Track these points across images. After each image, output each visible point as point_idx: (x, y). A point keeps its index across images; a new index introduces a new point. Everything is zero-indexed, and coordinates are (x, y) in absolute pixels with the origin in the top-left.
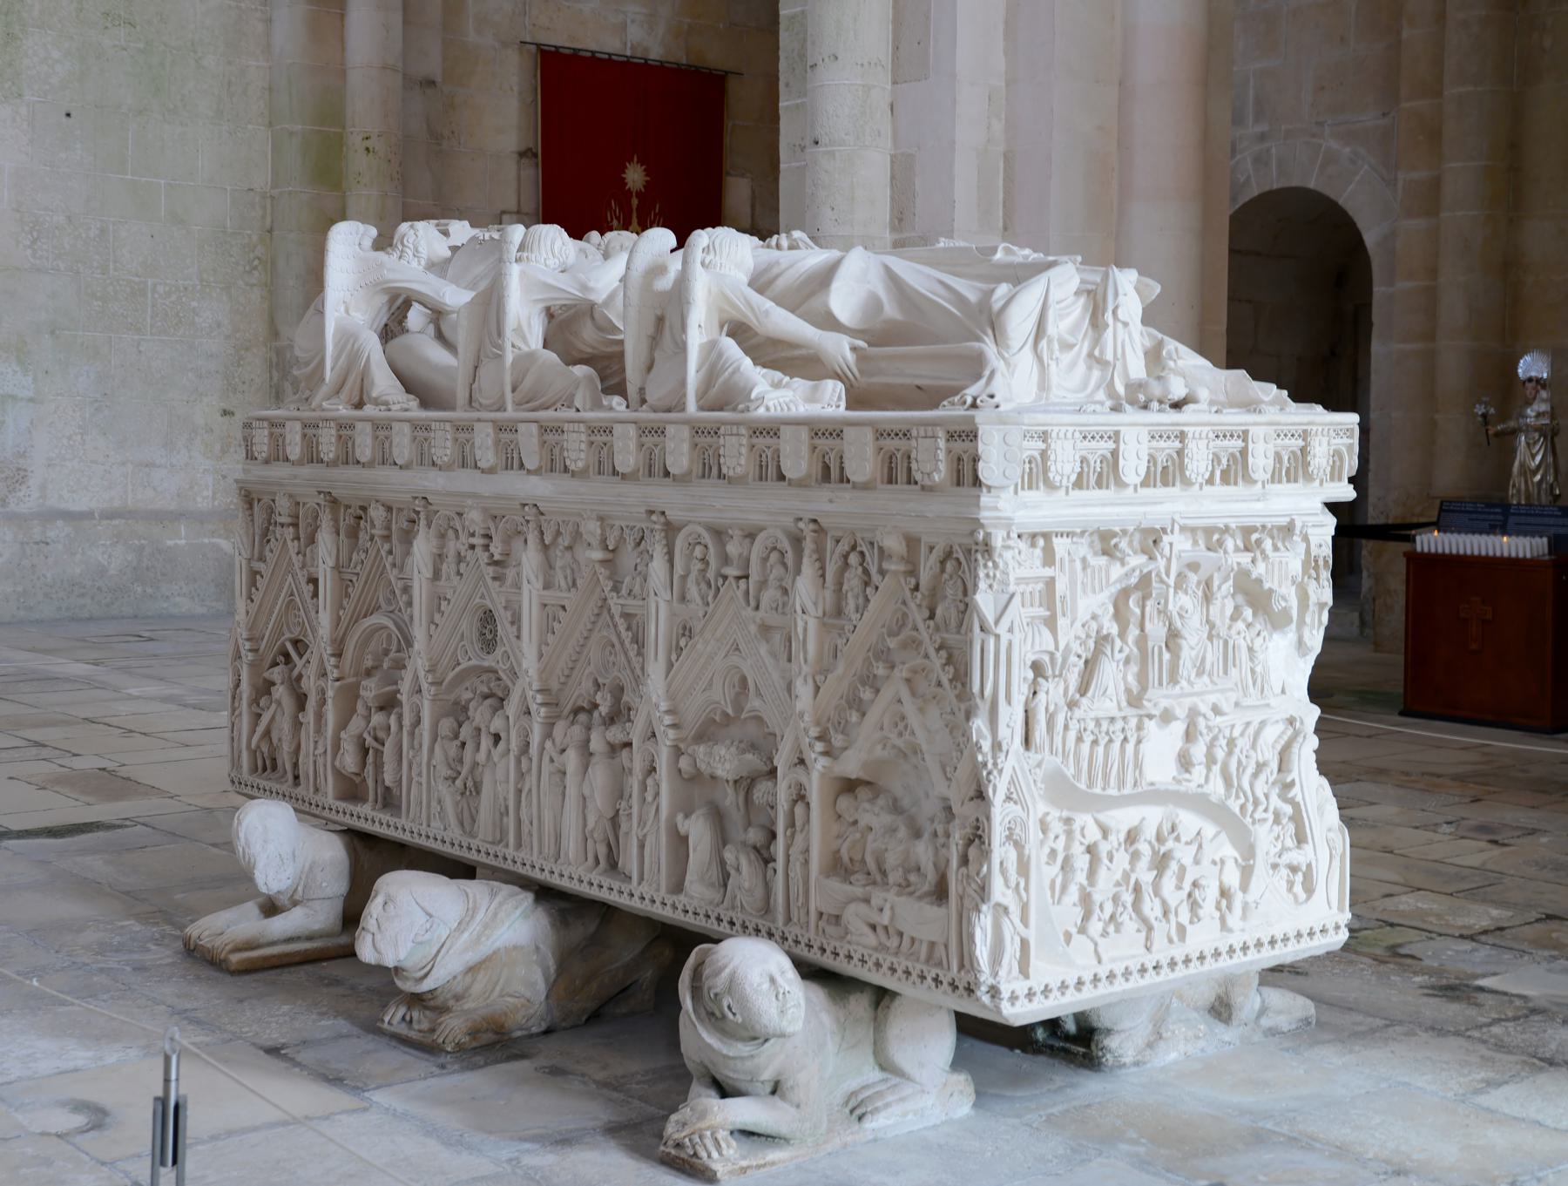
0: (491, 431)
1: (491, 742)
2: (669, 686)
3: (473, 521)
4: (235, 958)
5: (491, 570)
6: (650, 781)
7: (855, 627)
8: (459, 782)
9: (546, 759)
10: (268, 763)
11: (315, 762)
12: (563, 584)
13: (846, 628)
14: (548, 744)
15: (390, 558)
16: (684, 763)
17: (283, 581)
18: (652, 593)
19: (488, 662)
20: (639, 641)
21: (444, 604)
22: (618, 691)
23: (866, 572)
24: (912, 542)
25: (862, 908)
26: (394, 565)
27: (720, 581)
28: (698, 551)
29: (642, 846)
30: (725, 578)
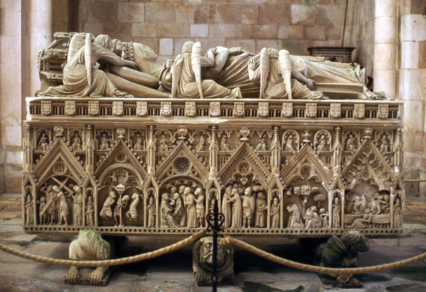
0: (194, 104)
1: (194, 198)
2: (280, 174)
3: (182, 132)
4: (104, 280)
5: (190, 147)
6: (275, 199)
7: (355, 153)
8: (176, 212)
9: (224, 199)
10: (44, 220)
11: (86, 216)
12: (226, 148)
13: (352, 153)
14: (225, 195)
15: (129, 146)
16: (289, 193)
17: (55, 156)
18: (276, 148)
19: (185, 174)
20: (267, 162)
21: (163, 158)
22: (250, 177)
23: (356, 139)
24: (374, 131)
25: (361, 219)
26: (130, 148)
27: (302, 144)
28: (291, 136)
29: (271, 217)
30: (304, 143)
